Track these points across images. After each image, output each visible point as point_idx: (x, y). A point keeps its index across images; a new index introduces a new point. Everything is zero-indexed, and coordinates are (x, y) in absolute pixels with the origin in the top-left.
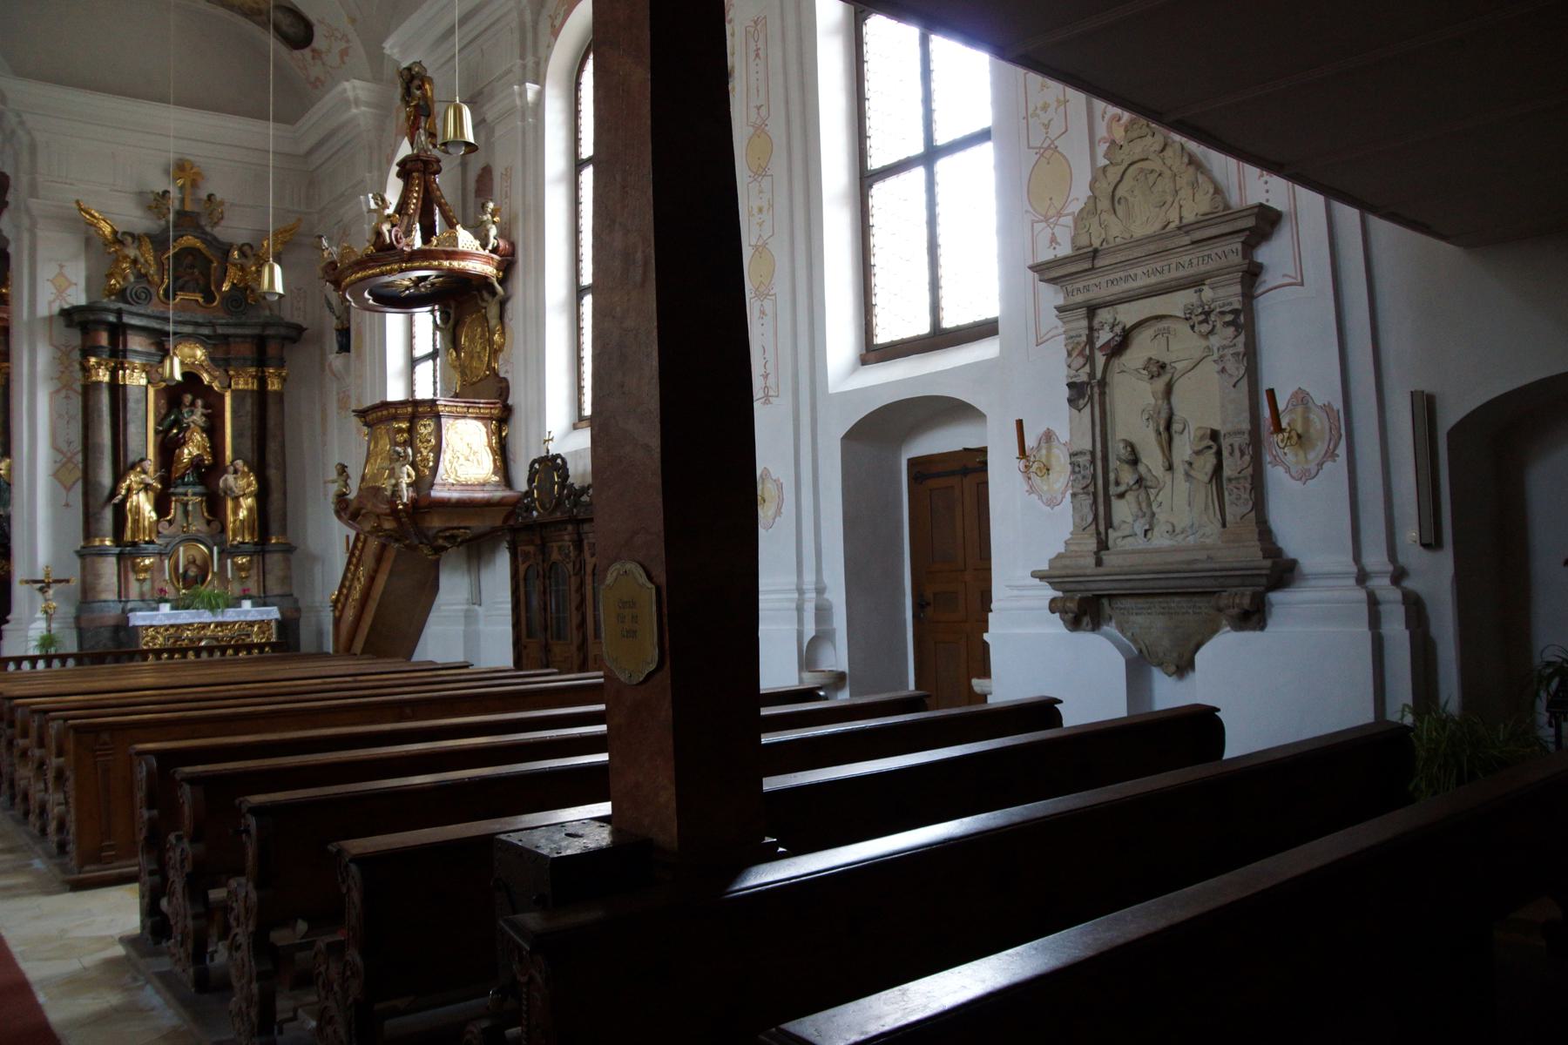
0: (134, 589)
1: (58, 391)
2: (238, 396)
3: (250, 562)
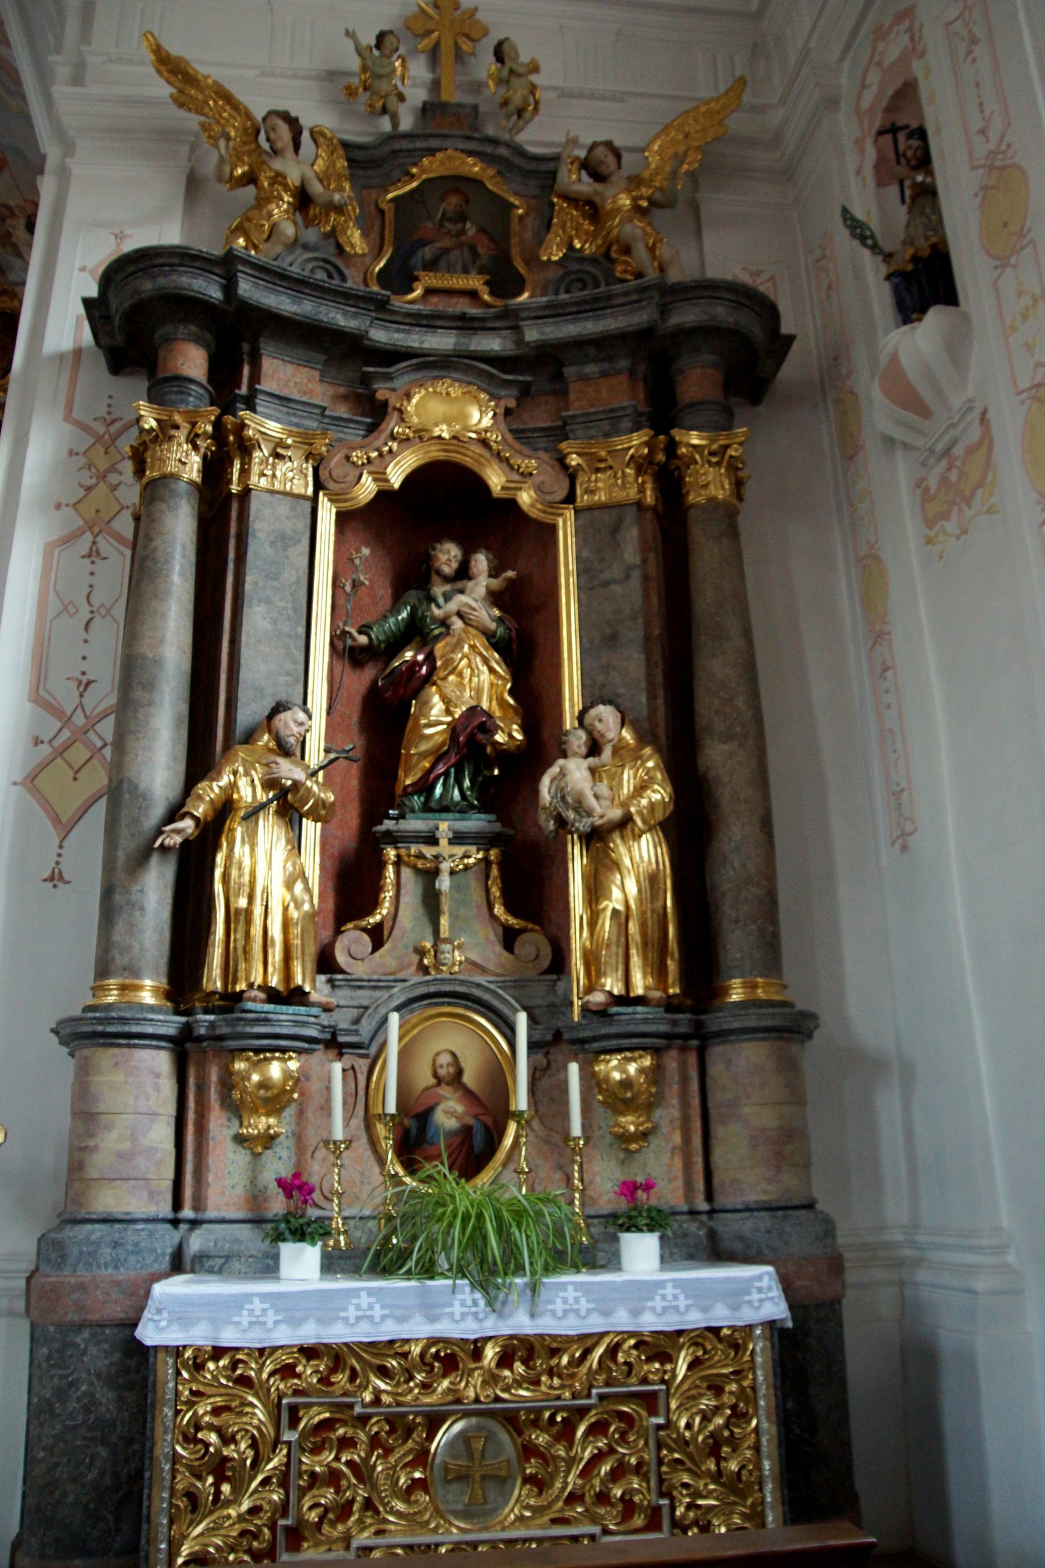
0: (227, 1177)
1: (68, 540)
2: (600, 526)
3: (655, 1075)
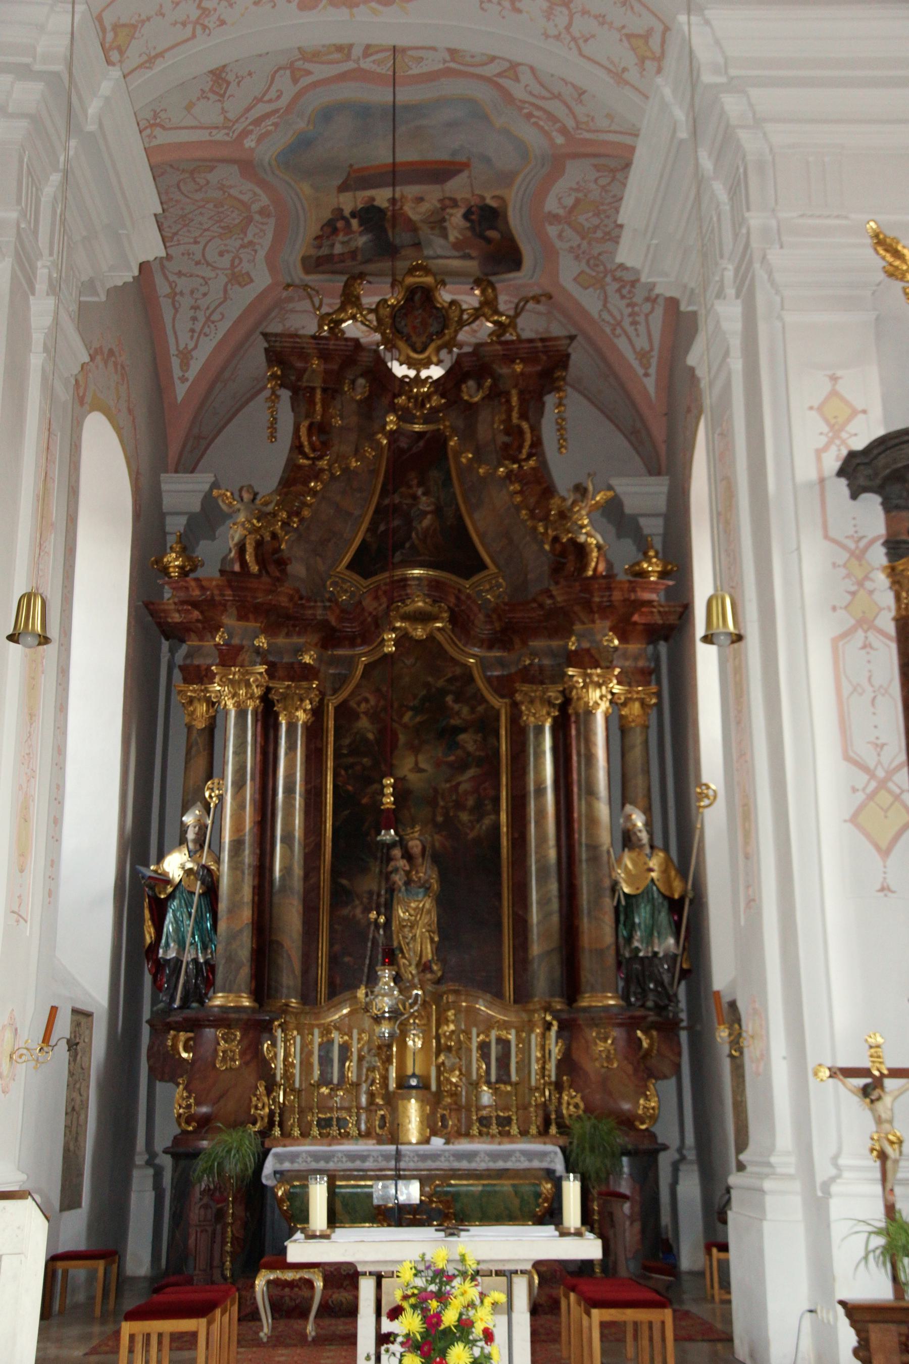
1: (846, 635)
